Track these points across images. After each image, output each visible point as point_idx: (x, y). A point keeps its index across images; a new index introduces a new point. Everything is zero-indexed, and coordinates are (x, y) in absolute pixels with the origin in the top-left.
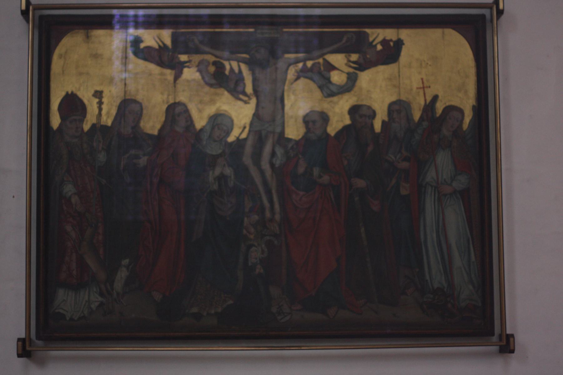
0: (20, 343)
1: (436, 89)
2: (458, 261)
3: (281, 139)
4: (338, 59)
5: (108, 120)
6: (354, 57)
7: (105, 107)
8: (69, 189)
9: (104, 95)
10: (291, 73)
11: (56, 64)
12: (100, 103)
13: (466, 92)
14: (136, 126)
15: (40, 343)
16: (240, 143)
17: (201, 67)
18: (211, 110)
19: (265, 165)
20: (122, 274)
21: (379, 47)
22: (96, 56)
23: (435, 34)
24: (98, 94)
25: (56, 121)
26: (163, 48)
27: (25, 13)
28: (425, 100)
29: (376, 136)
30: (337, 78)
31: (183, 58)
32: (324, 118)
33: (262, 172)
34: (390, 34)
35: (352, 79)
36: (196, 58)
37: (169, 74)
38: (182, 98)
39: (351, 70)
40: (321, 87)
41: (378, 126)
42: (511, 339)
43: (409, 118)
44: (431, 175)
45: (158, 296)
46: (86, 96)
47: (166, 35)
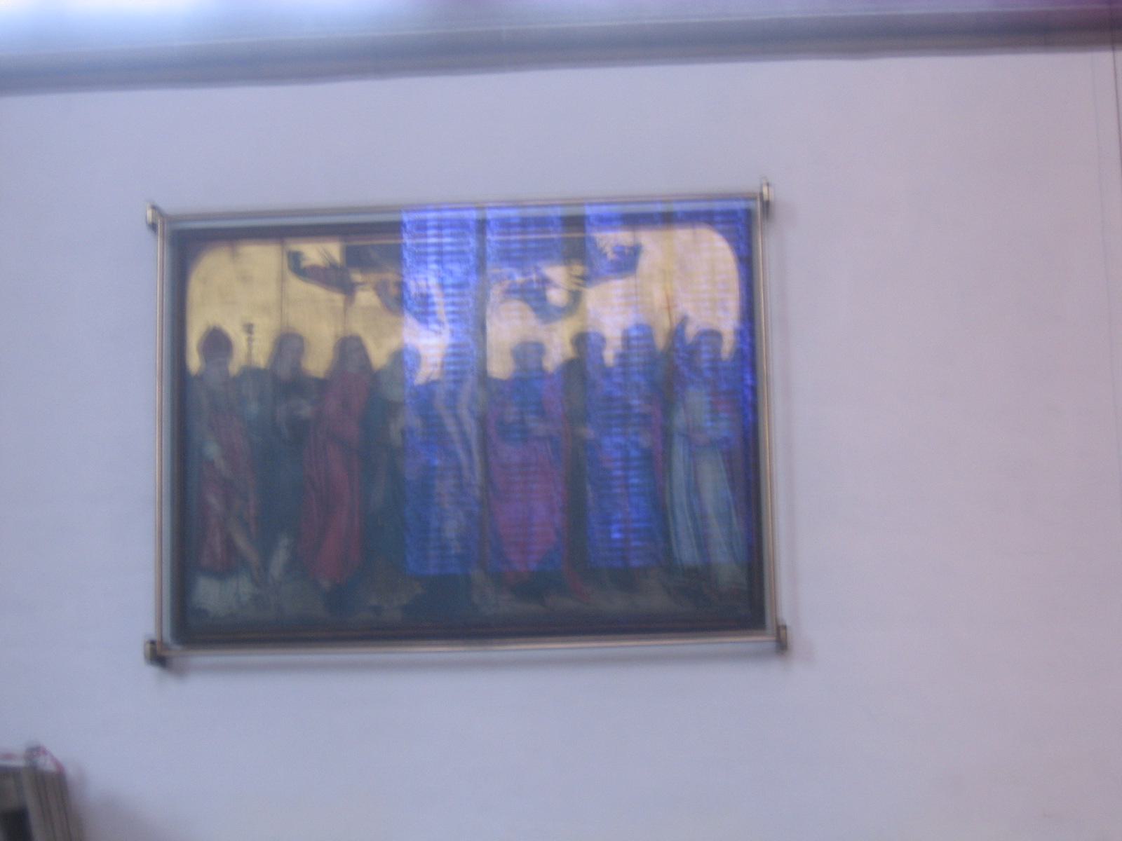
0: (148, 646)
1: (686, 306)
2: (717, 531)
3: (484, 378)
4: (557, 273)
5: (261, 358)
6: (578, 269)
7: (255, 344)
8: (212, 450)
9: (256, 329)
10: (496, 292)
11: (196, 289)
12: (250, 340)
13: (725, 309)
14: (297, 369)
15: (177, 648)
16: (430, 386)
17: (380, 289)
18: (392, 343)
19: (464, 413)
20: (280, 558)
21: (611, 256)
22: (245, 279)
23: (682, 236)
24: (249, 329)
25: (194, 362)
26: (333, 266)
27: (153, 227)
28: (671, 323)
29: (607, 373)
30: (556, 296)
31: (357, 277)
32: (539, 349)
33: (459, 422)
34: (623, 237)
35: (576, 298)
36: (373, 277)
37: (338, 298)
38: (358, 327)
39: (574, 287)
40: (535, 310)
41: (609, 356)
42: (782, 632)
43: (651, 346)
44: (680, 420)
45: (326, 584)
46: (234, 330)
47: (333, 250)
